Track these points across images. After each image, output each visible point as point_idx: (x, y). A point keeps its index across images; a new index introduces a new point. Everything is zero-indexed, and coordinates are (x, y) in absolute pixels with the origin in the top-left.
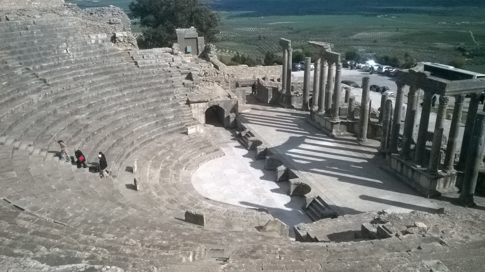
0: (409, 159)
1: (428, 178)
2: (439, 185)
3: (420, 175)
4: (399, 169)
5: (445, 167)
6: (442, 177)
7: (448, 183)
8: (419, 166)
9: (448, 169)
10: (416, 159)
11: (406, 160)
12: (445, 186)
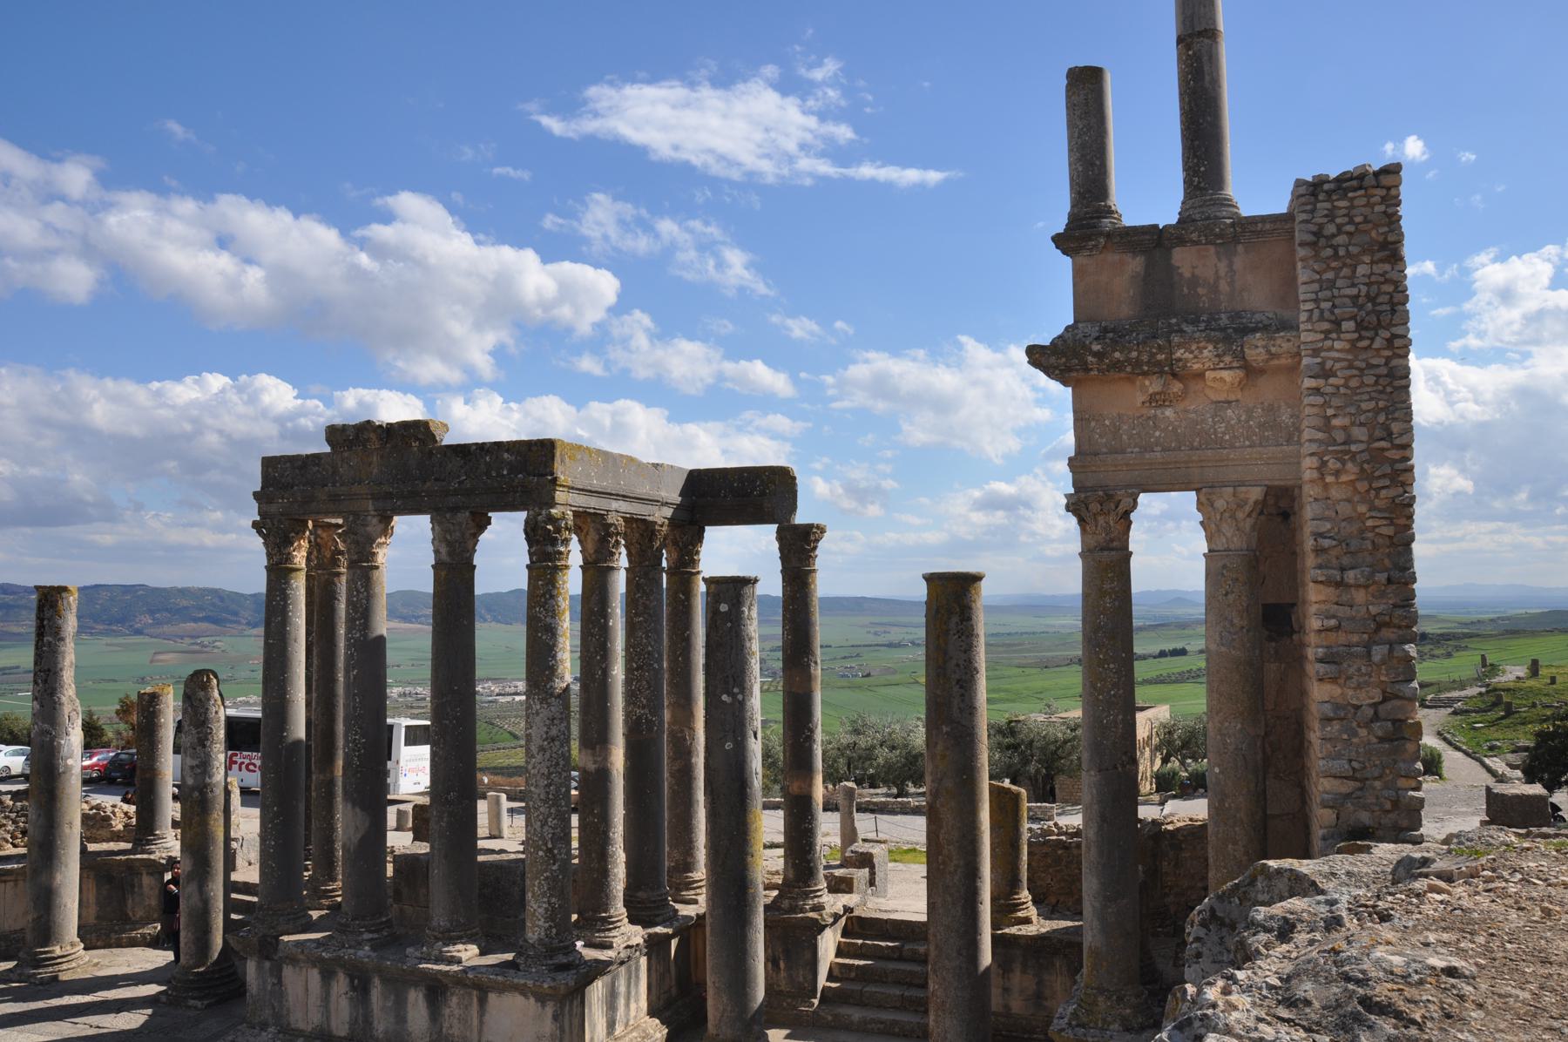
0: (393, 939)
1: (541, 999)
2: (593, 1027)
3: (483, 1001)
4: (341, 1019)
5: (595, 922)
6: (600, 968)
7: (621, 1002)
8: (468, 953)
9: (607, 924)
10: (440, 917)
11: (373, 949)
12: (611, 1025)
